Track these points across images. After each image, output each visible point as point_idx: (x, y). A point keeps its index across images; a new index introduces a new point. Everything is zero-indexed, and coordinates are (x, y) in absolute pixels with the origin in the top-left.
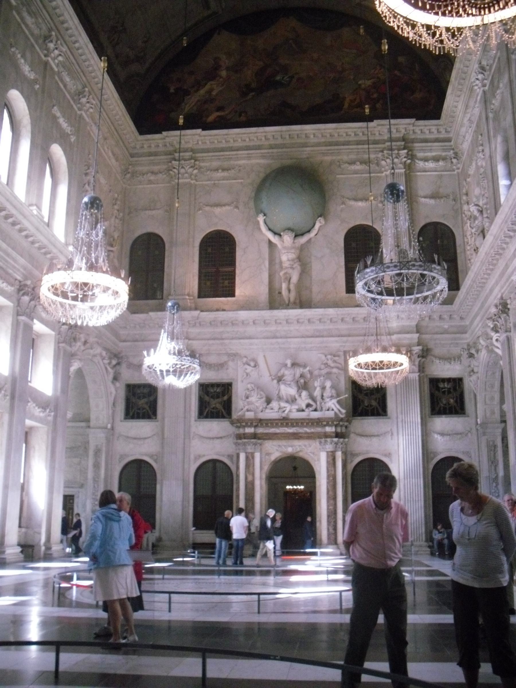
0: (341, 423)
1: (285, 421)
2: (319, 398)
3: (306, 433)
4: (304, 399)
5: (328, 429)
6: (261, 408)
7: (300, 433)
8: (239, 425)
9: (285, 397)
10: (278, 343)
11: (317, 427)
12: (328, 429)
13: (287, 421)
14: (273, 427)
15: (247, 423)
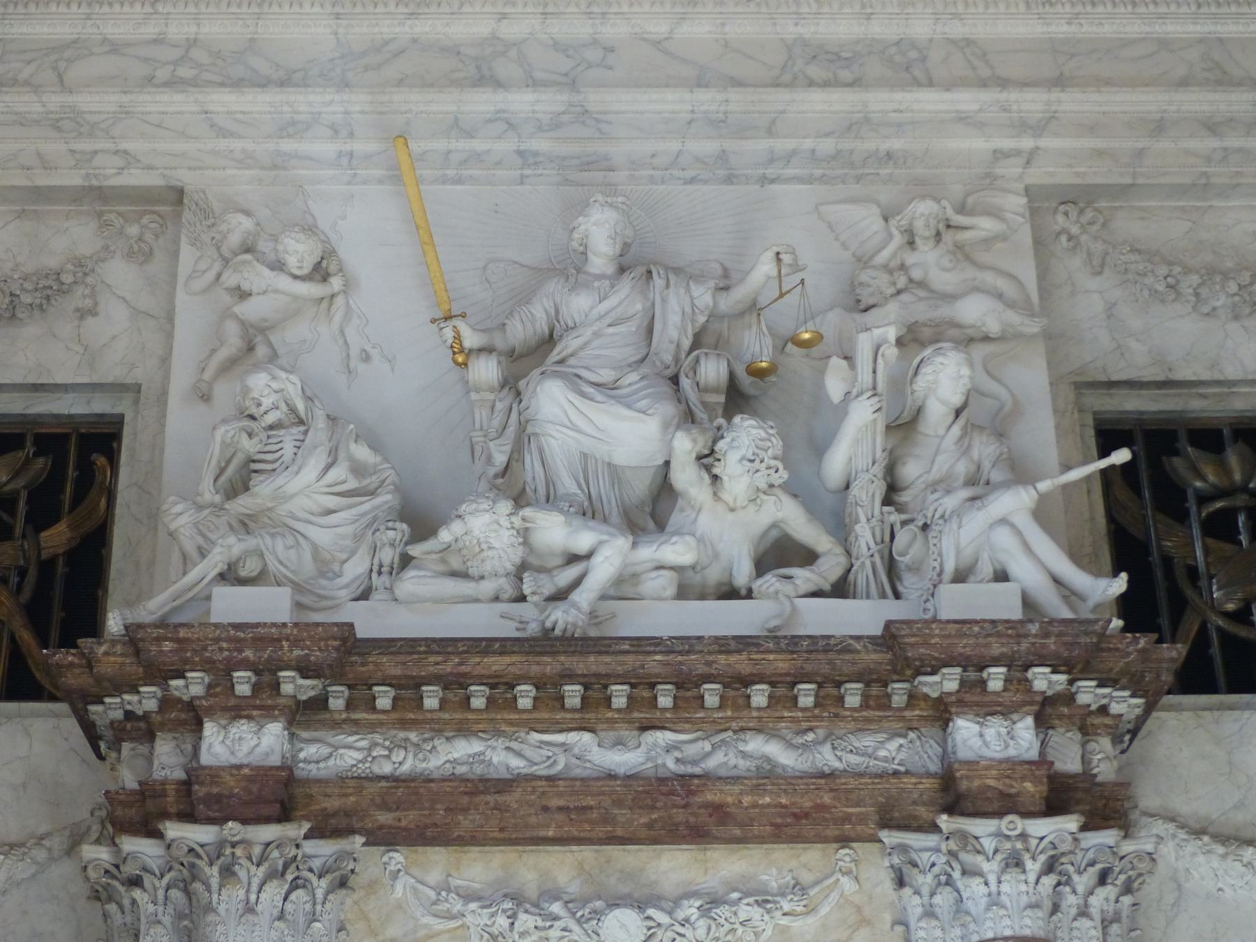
0: (1088, 693)
1: (573, 669)
2: (868, 491)
3: (768, 775)
4: (737, 499)
5: (974, 738)
6: (356, 568)
7: (705, 776)
8: (147, 700)
9: (568, 485)
10: (508, 123)
11: (864, 726)
12: (974, 738)
13: (593, 663)
14: (464, 730)
15: (222, 674)
